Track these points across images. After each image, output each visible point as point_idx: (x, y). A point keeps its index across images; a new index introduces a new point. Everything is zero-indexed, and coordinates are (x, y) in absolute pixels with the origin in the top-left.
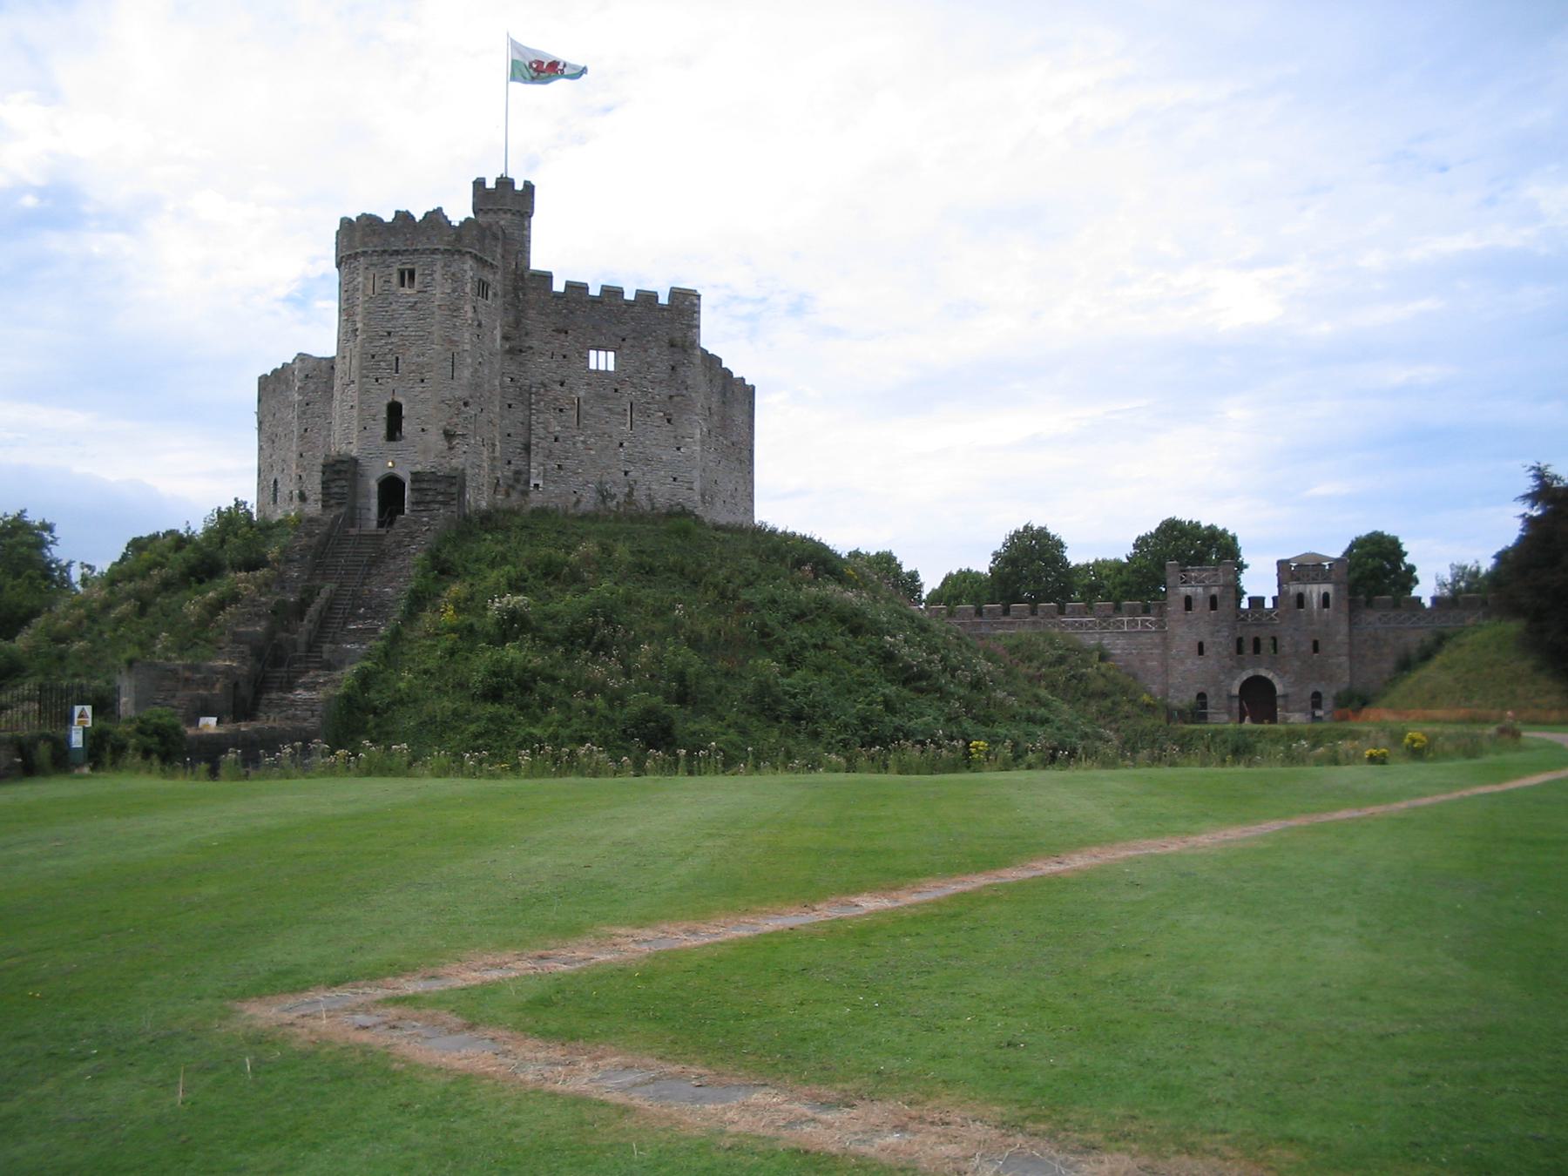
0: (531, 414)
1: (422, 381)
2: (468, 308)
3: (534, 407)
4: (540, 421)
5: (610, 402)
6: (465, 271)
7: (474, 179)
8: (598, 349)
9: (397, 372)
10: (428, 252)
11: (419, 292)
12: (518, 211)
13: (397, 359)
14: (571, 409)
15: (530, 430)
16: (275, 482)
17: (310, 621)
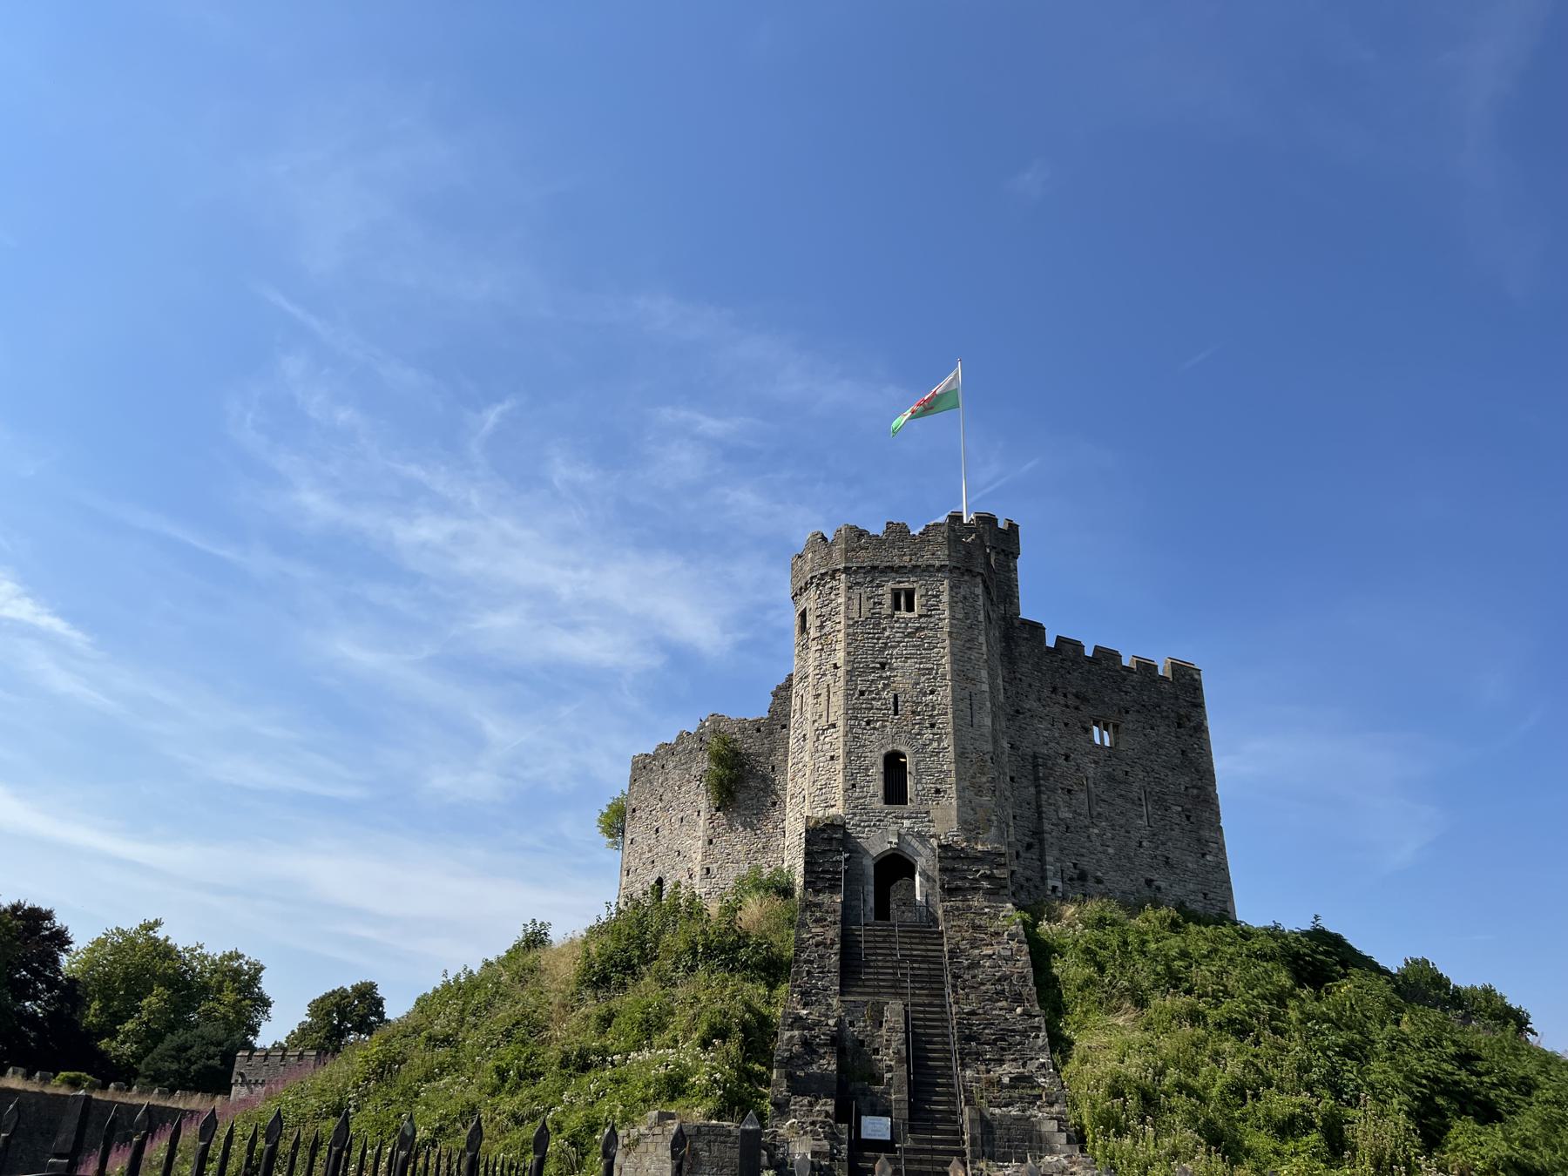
0: (1039, 793)
1: (932, 726)
2: (982, 639)
4: (1050, 801)
5: (1122, 786)
6: (978, 596)
9: (896, 713)
10: (932, 569)
12: (1003, 551)
13: (896, 697)
14: (1082, 790)
15: (1040, 813)
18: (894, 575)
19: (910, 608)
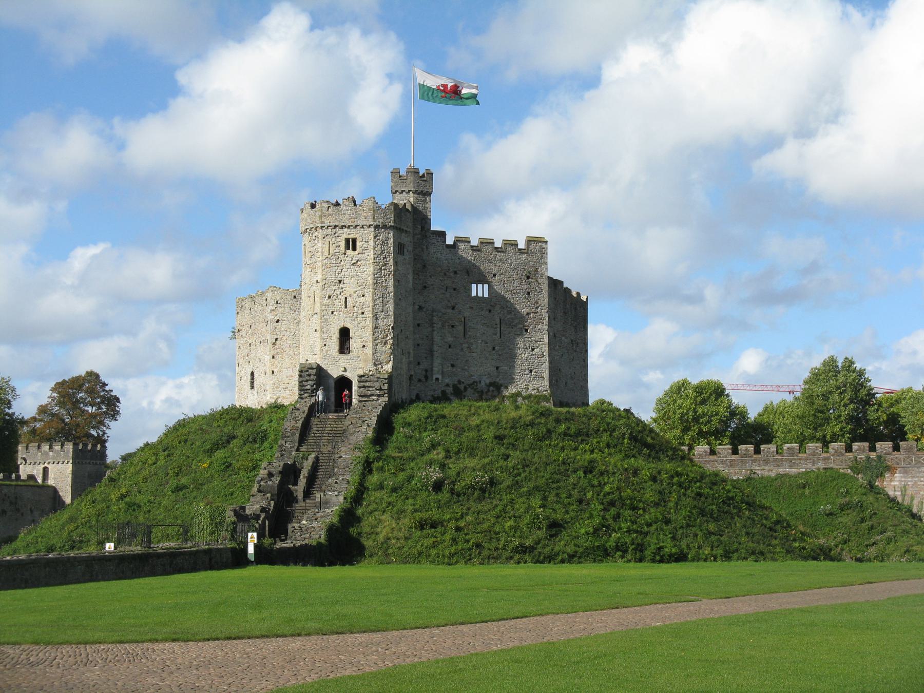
0: (433, 331)
1: (363, 313)
2: (391, 262)
3: (435, 325)
7: (391, 170)
8: (477, 283)
9: (346, 307)
11: (359, 254)
13: (346, 298)
15: (433, 341)
16: (252, 374)
17: (304, 478)
18: (346, 230)
19: (354, 249)
